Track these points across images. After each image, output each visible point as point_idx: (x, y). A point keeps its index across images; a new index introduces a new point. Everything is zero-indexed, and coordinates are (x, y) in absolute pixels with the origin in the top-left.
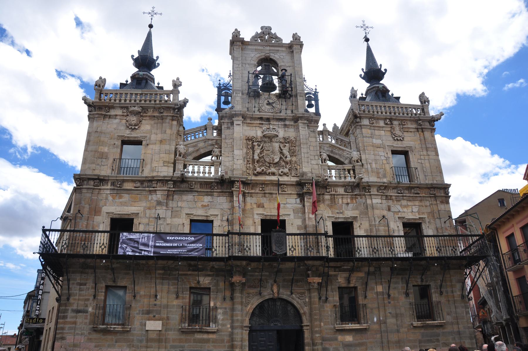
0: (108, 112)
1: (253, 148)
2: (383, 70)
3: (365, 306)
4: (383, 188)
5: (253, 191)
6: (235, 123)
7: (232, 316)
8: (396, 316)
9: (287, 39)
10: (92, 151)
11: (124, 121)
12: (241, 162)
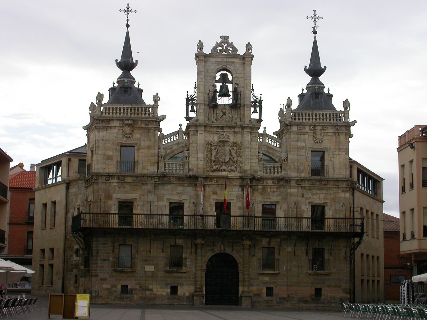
1: (211, 150)
2: (323, 67)
3: (278, 260)
4: (300, 181)
6: (199, 132)
7: (196, 263)
8: (298, 267)
9: (242, 51)
10: (101, 155)
11: (121, 131)
12: (202, 162)
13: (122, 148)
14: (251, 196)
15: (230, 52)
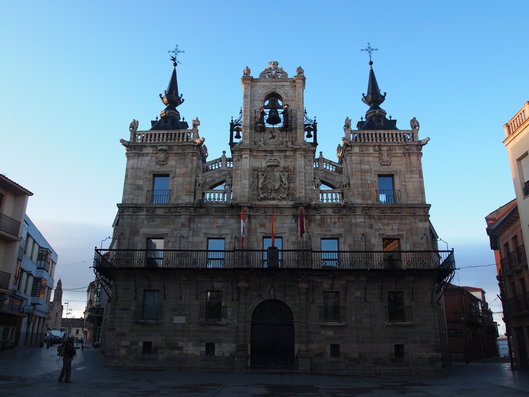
0: (142, 151)
1: (258, 177)
5: (257, 214)
6: (244, 156)
9: (292, 74)
10: (130, 184)
11: (154, 158)
12: (247, 190)
13: (156, 178)
14: (307, 229)
15: (279, 77)
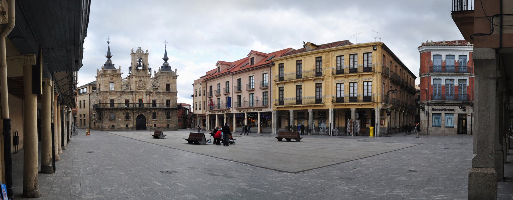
4: (163, 93)
9: (145, 52)
